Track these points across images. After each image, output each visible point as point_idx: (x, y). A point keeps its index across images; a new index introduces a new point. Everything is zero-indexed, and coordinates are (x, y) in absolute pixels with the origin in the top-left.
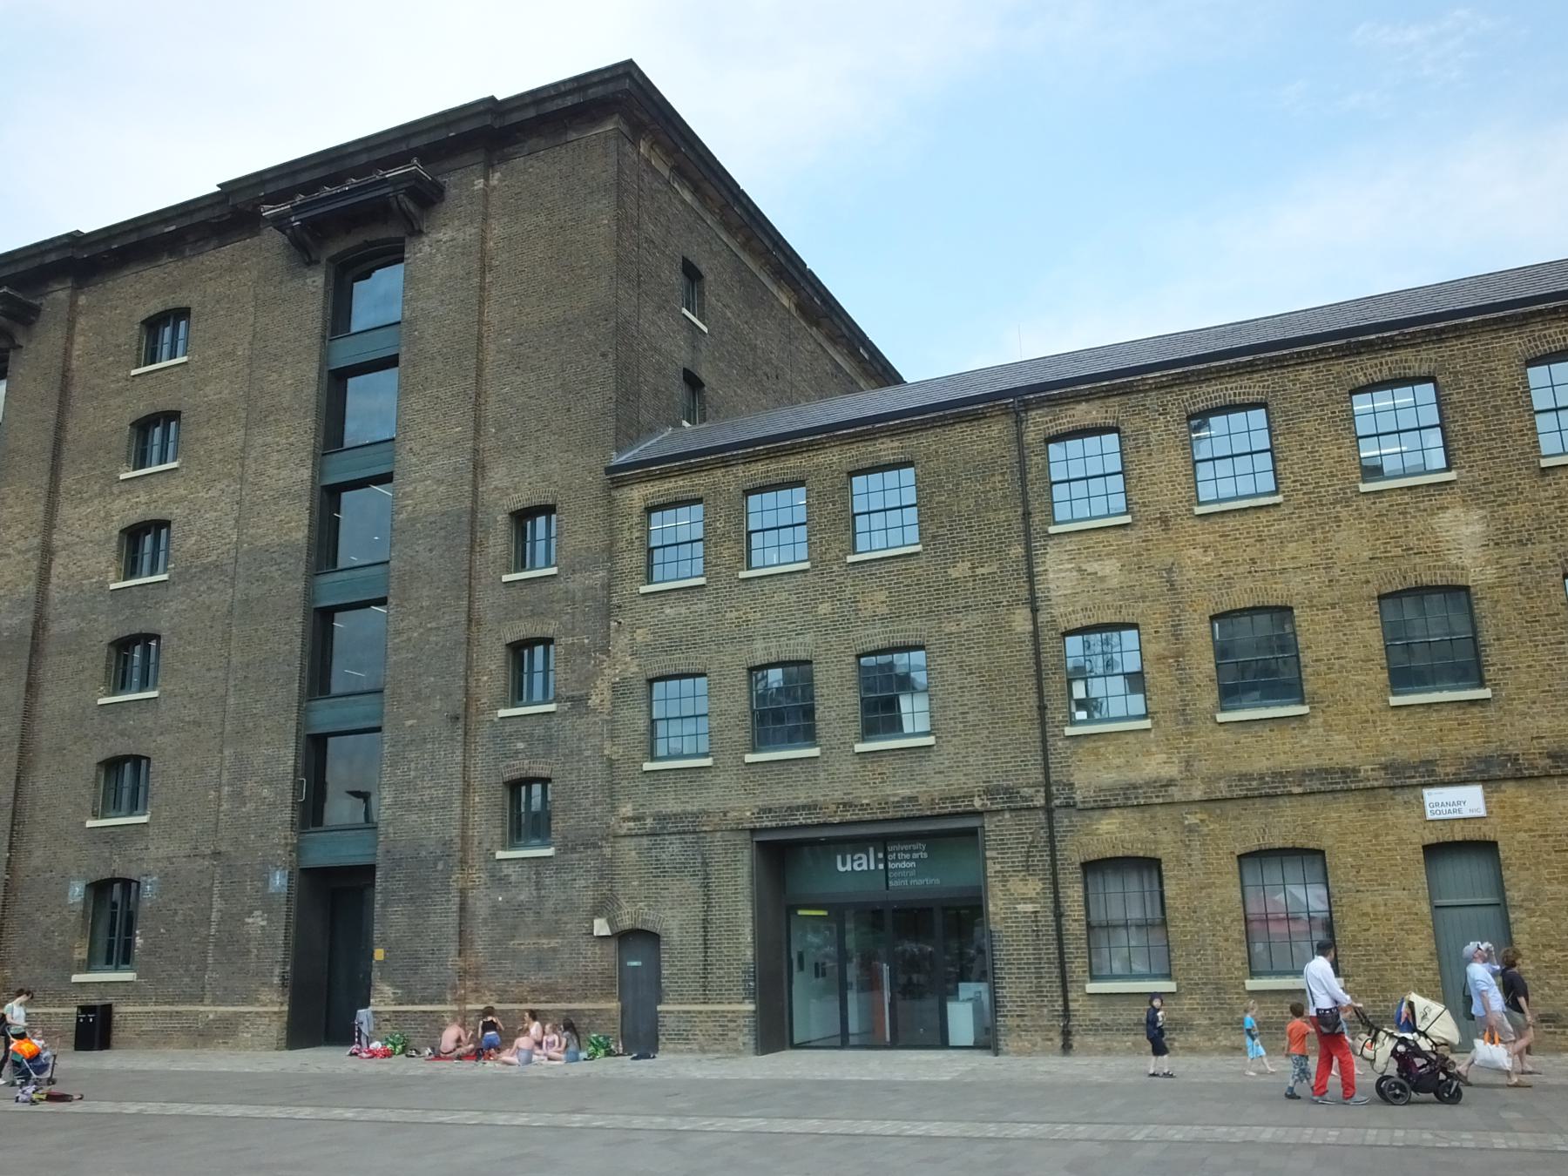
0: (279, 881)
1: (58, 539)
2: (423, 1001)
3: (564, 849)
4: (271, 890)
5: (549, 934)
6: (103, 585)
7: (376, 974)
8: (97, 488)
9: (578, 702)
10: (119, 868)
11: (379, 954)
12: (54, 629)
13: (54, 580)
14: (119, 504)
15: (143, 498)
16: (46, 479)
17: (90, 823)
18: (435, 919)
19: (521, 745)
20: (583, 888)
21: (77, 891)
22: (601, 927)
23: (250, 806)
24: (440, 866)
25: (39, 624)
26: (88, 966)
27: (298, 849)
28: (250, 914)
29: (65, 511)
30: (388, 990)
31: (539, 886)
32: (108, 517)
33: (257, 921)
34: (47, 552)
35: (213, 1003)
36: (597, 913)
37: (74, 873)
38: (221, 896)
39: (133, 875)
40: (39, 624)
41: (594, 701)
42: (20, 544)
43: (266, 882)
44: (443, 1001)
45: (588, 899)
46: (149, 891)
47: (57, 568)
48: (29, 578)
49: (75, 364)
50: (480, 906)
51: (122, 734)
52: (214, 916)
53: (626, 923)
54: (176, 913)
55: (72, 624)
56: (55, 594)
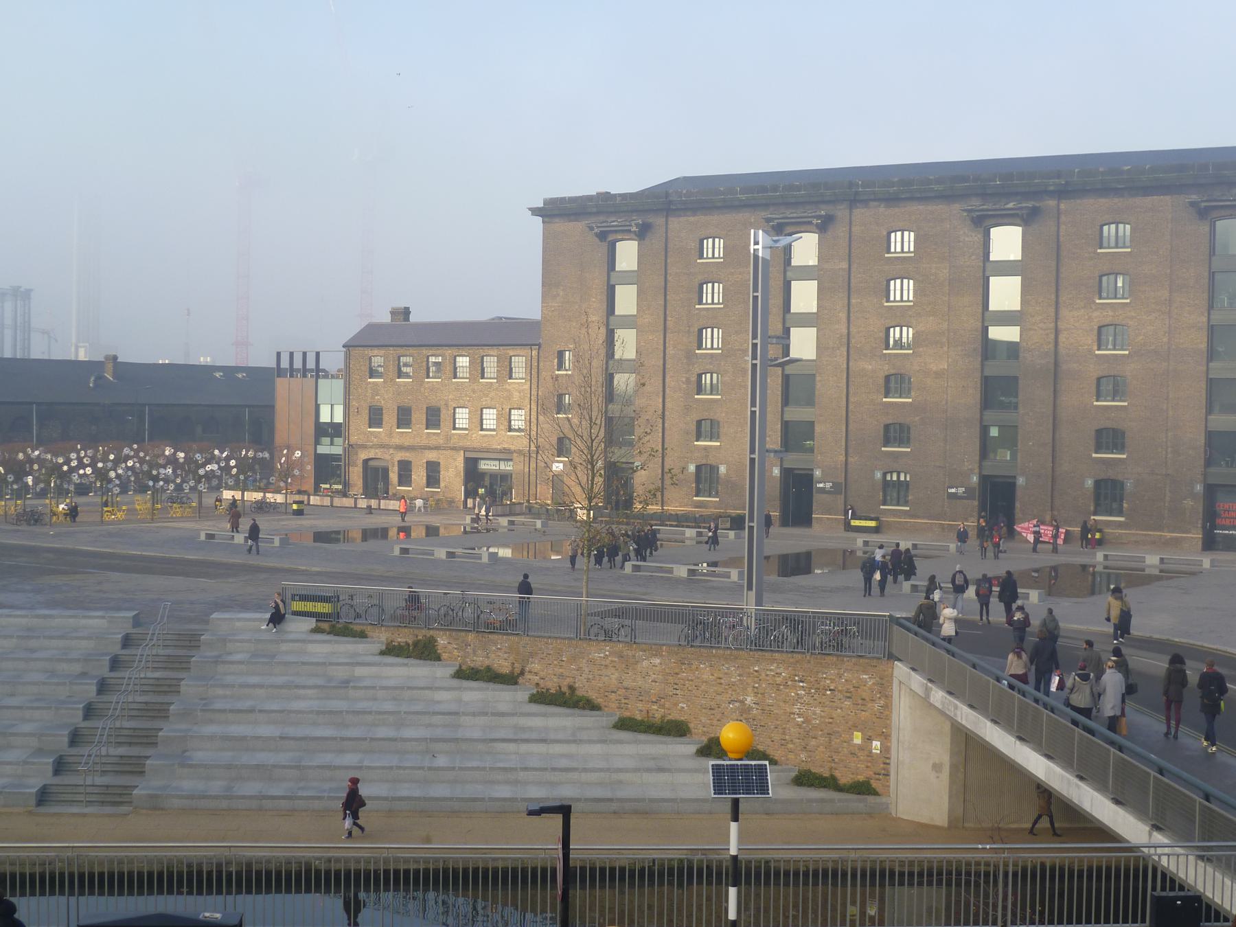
0: (1199, 488)
1: (1061, 325)
6: (1090, 351)
10: (1111, 474)
14: (1096, 314)
15: (1110, 313)
16: (1053, 297)
17: (1094, 455)
21: (1089, 483)
25: (1056, 364)
26: (1095, 514)
27: (1205, 475)
29: (1064, 312)
32: (1090, 319)
33: (1189, 503)
34: (1057, 332)
39: (1120, 478)
40: (1056, 364)
42: (1041, 325)
46: (1129, 485)
47: (1062, 338)
49: (1061, 239)
52: (1167, 499)
56: (1062, 351)
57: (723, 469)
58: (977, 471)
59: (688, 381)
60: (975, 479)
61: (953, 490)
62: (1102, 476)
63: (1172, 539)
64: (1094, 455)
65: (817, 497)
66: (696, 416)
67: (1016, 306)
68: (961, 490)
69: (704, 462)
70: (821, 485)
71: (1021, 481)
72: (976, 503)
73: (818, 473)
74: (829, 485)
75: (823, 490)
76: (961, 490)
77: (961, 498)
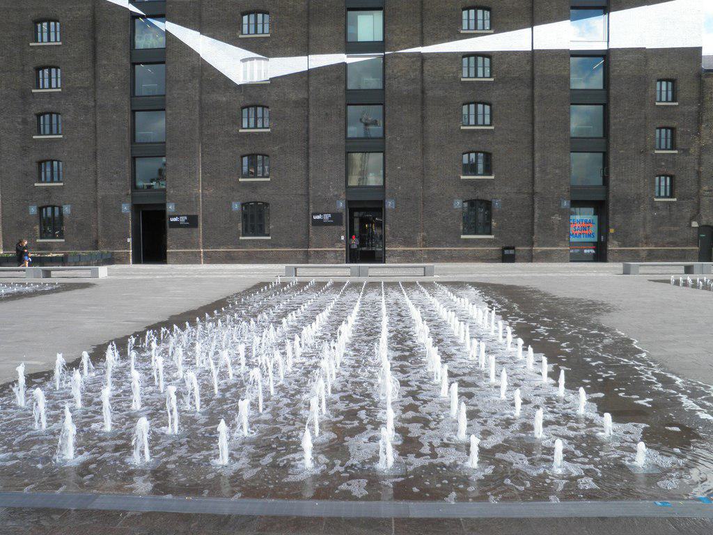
2: (630, 246)
3: (679, 199)
4: (562, 207)
5: (674, 225)
7: (610, 237)
8: (446, 34)
9: (686, 151)
10: (480, 195)
11: (612, 231)
12: (430, 94)
13: (426, 72)
16: (419, 26)
17: (462, 177)
18: (633, 220)
19: (663, 164)
20: (687, 212)
22: (695, 224)
23: (549, 176)
24: (636, 202)
28: (553, 215)
30: (616, 242)
31: (670, 210)
35: (538, 246)
36: (692, 219)
37: (456, 196)
38: (539, 208)
39: (488, 198)
40: (423, 92)
41: (692, 151)
43: (560, 205)
44: (638, 246)
45: (689, 215)
46: (497, 204)
48: (416, 70)
50: (649, 218)
51: (476, 142)
52: (536, 215)
53: (704, 223)
54: (512, 214)
55: (440, 93)
56: (428, 79)
57: (67, 209)
58: (343, 196)
59: (25, 122)
60: (341, 205)
61: (319, 217)
62: (472, 197)
63: (543, 252)
64: (462, 177)
65: (171, 232)
66: (35, 157)
67: (379, 38)
68: (327, 217)
69: (46, 203)
70: (175, 219)
71: (390, 204)
72: (343, 228)
73: (171, 208)
74: (183, 219)
75: (177, 225)
76: (327, 217)
77: (327, 224)
